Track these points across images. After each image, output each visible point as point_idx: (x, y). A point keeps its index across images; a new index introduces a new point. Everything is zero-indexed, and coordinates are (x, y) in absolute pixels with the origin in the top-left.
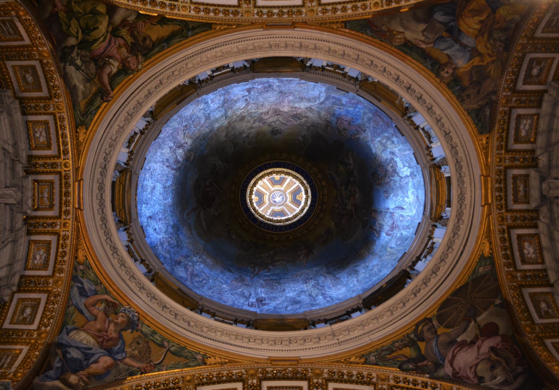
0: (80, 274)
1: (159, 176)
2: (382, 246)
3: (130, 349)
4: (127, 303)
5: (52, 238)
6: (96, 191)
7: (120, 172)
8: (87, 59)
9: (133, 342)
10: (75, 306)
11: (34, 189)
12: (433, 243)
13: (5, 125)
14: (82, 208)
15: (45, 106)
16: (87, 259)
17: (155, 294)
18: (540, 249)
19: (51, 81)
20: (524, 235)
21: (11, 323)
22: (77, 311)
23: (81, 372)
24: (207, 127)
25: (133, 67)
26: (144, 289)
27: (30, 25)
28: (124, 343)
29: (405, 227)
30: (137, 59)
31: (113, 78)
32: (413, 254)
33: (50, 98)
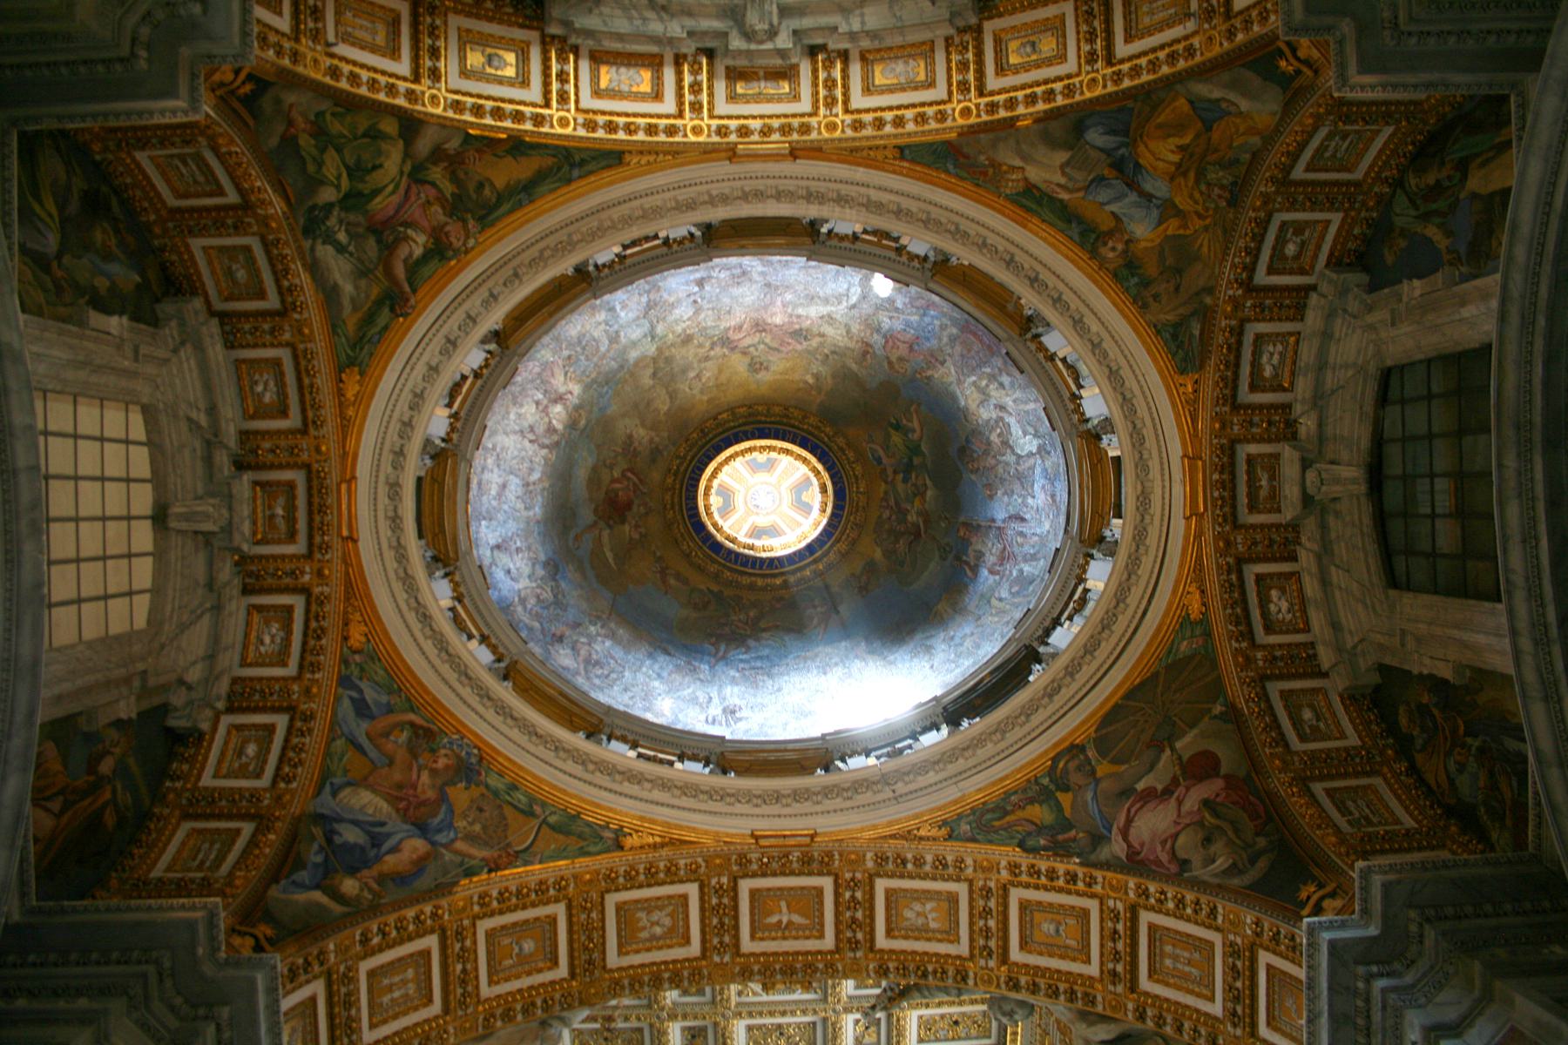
0: (356, 672)
2: (982, 596)
5: (298, 602)
7: (432, 457)
8: (361, 230)
9: (470, 808)
11: (254, 499)
12: (1086, 591)
13: (190, 370)
15: (272, 331)
18: (1301, 604)
19: (285, 277)
20: (1271, 575)
21: (216, 776)
23: (365, 872)
25: (457, 244)
26: (489, 698)
27: (239, 165)
28: (452, 812)
30: (465, 227)
31: (414, 268)
33: (282, 313)
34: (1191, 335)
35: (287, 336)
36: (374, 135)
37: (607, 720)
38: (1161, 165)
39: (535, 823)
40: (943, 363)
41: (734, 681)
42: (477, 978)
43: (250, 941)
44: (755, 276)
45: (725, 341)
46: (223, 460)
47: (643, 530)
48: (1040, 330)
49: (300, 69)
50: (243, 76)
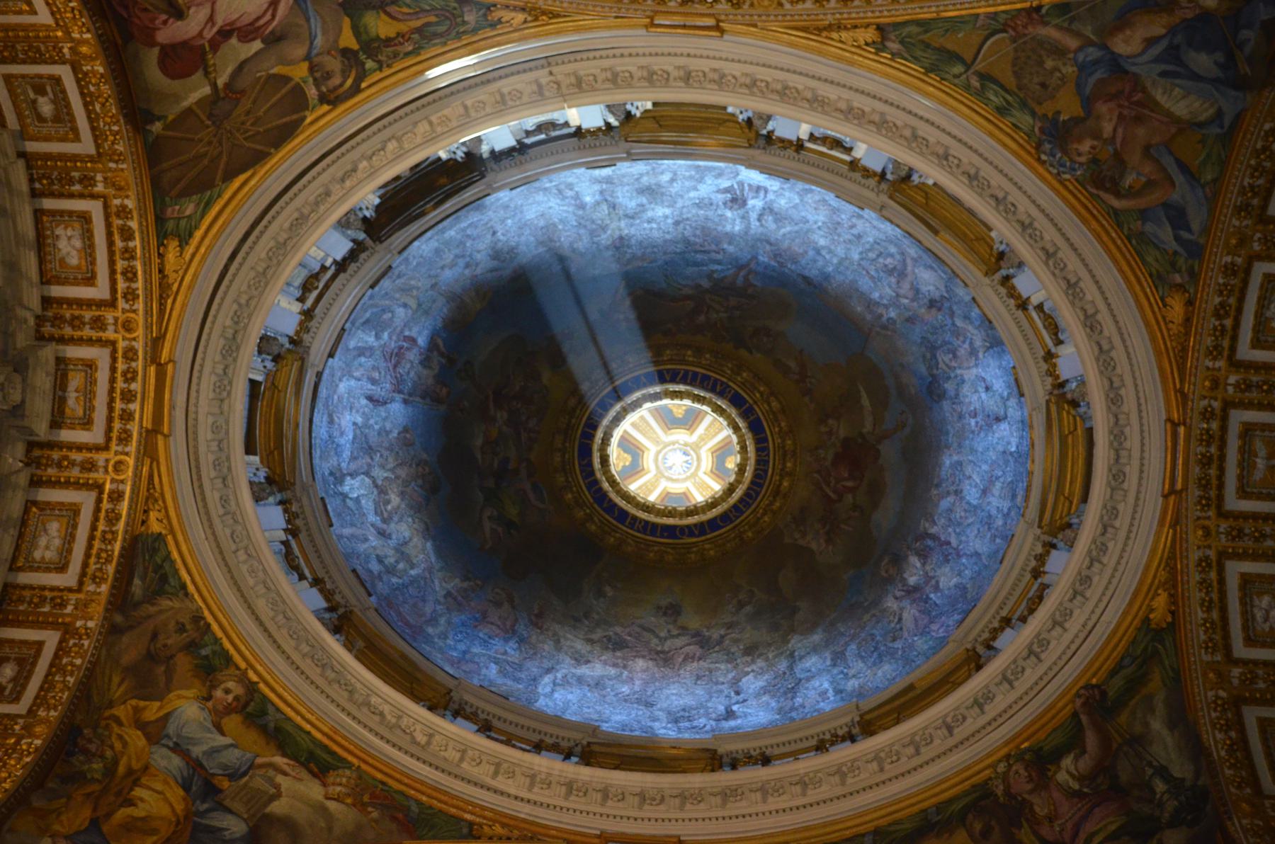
0: (1181, 262)
1: (971, 520)
2: (426, 313)
3: (1064, 71)
4: (1066, 187)
6: (1132, 471)
12: (301, 299)
14: (1169, 425)
16: (1162, 299)
17: (997, 209)
20: (76, 282)
23: (1190, 15)
24: (843, 634)
25: (1018, 767)
26: (1022, 224)
28: (1079, 87)
29: (368, 354)
32: (354, 282)
34: (143, 579)
37: (884, 198)
38: (159, 787)
39: (979, 66)
40: (448, 594)
41: (731, 238)
44: (661, 715)
45: (705, 643)
47: (823, 429)
48: (327, 616)
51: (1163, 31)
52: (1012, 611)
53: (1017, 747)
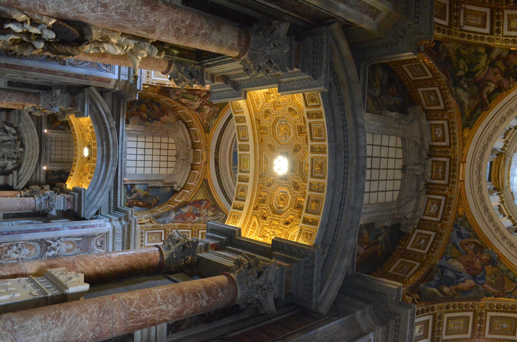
0: (459, 223)
3: (489, 279)
5: (443, 198)
7: (497, 155)
10: (453, 243)
11: (433, 166)
15: (442, 115)
16: (465, 214)
19: (446, 99)
21: (411, 247)
22: (454, 246)
23: (452, 286)
25: (506, 86)
26: (506, 238)
28: (485, 273)
30: (509, 80)
33: (445, 110)
35: (446, 117)
36: (477, 53)
42: (485, 330)
43: (412, 298)
46: (424, 154)
49: (450, 37)
50: (432, 41)
51: (460, 284)
52: (514, 131)
53: (507, 92)
